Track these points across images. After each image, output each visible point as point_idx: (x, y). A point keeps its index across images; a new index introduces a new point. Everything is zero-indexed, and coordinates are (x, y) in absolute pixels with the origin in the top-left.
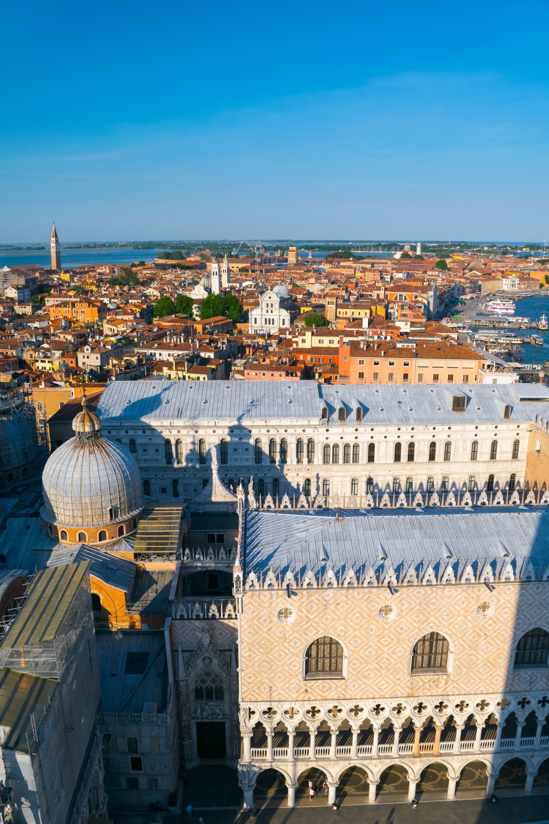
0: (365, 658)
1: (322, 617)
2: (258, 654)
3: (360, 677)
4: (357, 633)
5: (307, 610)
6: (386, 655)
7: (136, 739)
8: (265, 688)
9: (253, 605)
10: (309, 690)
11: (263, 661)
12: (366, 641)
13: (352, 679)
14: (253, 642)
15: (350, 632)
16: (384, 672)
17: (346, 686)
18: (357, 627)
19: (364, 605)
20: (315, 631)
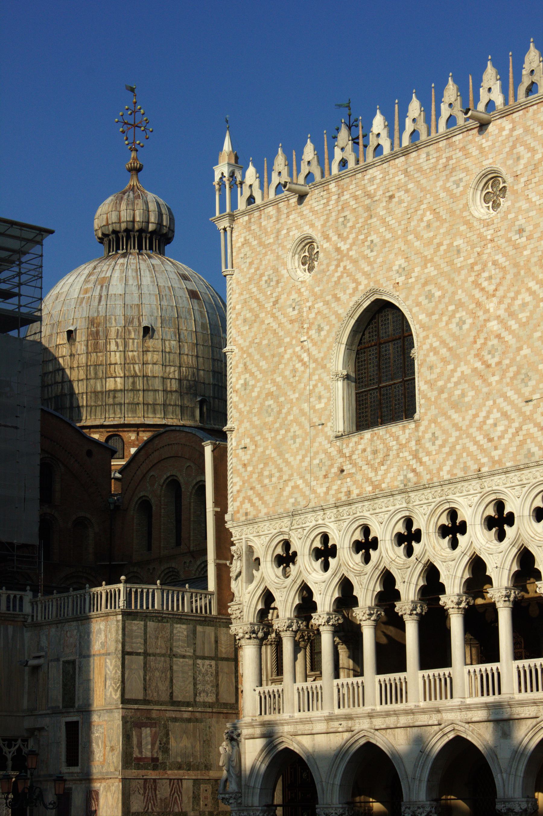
0: (453, 344)
4: (431, 270)
6: (494, 325)
10: (347, 467)
16: (494, 379)
17: (418, 441)
18: (428, 252)
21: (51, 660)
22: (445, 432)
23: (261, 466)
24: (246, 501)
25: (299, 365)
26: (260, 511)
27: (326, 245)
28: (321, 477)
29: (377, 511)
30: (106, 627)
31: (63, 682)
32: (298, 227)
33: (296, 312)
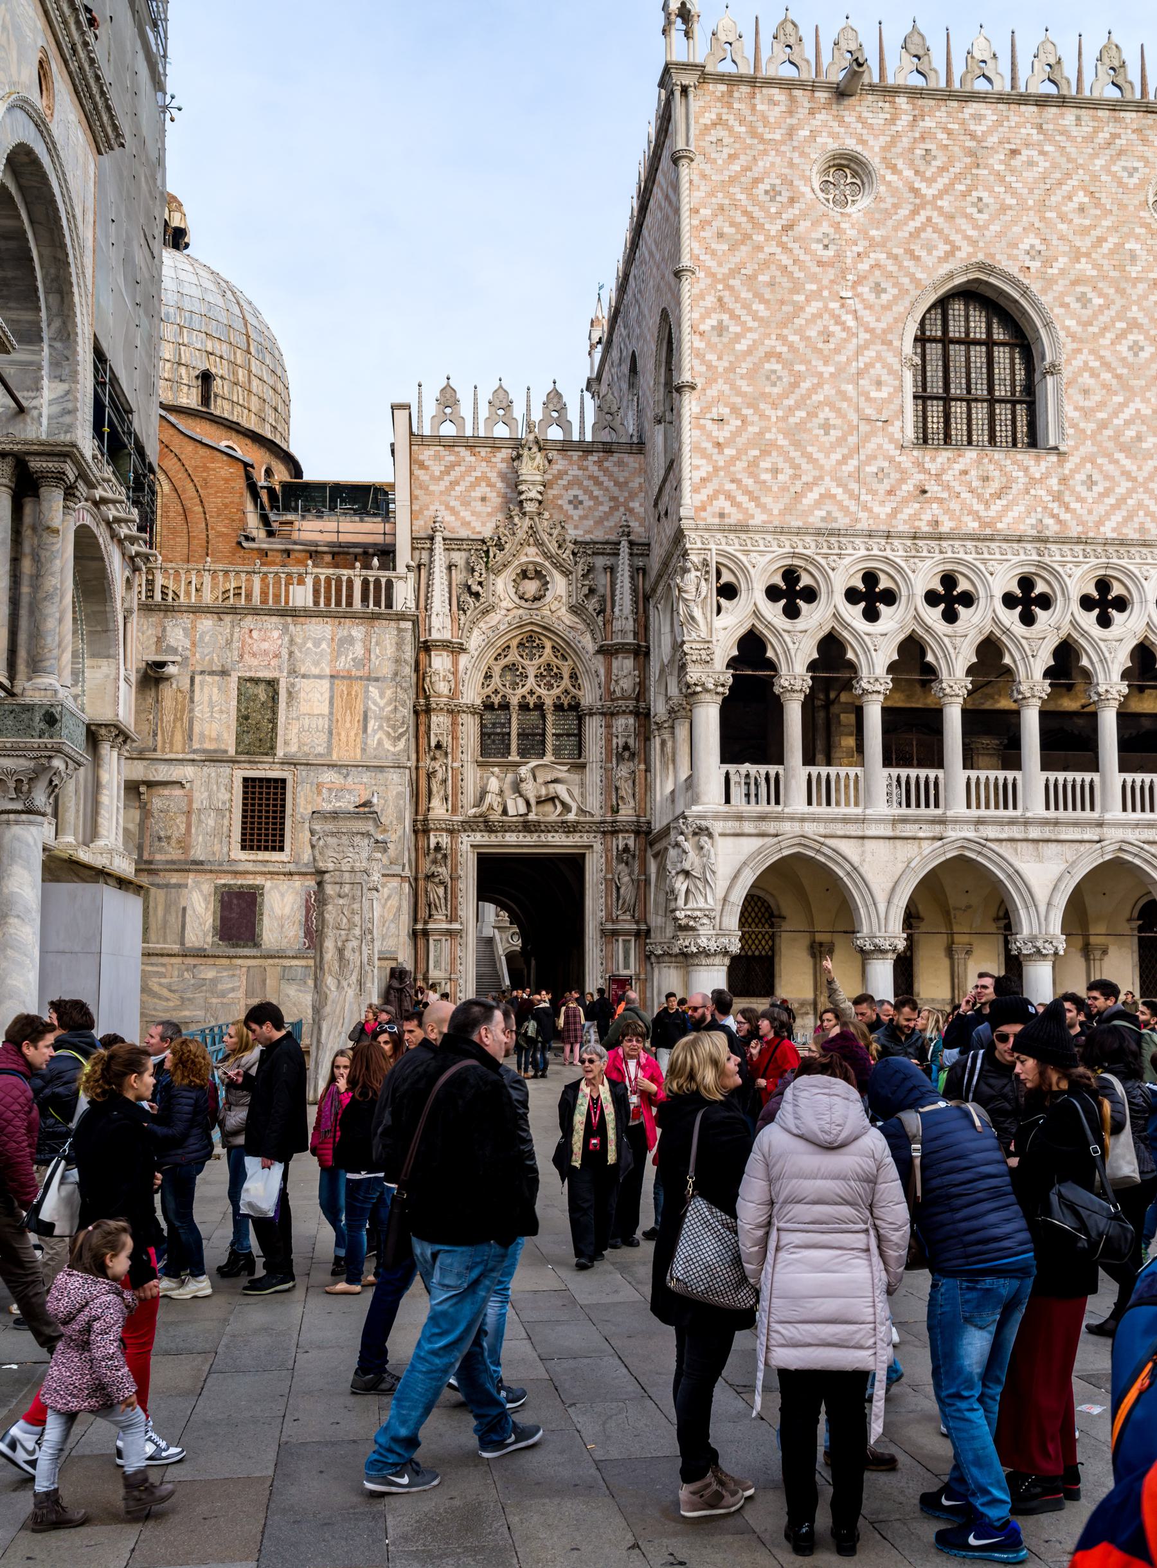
1: (964, 195)
2: (751, 324)
3: (1110, 445)
5: (911, 163)
7: (272, 684)
8: (775, 471)
9: (730, 129)
10: (933, 488)
11: (769, 355)
12: (1119, 302)
13: (1083, 451)
14: (735, 272)
15: (1062, 261)
17: (1063, 480)
18: (1084, 243)
19: (1099, 162)
20: (943, 248)
21: (202, 672)
22: (1107, 477)
23: (756, 453)
24: (722, 497)
25: (838, 328)
26: (752, 517)
27: (889, 177)
28: (882, 492)
29: (986, 556)
30: (368, 635)
31: (239, 710)
32: (834, 136)
33: (830, 253)
